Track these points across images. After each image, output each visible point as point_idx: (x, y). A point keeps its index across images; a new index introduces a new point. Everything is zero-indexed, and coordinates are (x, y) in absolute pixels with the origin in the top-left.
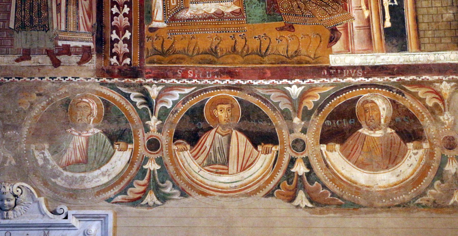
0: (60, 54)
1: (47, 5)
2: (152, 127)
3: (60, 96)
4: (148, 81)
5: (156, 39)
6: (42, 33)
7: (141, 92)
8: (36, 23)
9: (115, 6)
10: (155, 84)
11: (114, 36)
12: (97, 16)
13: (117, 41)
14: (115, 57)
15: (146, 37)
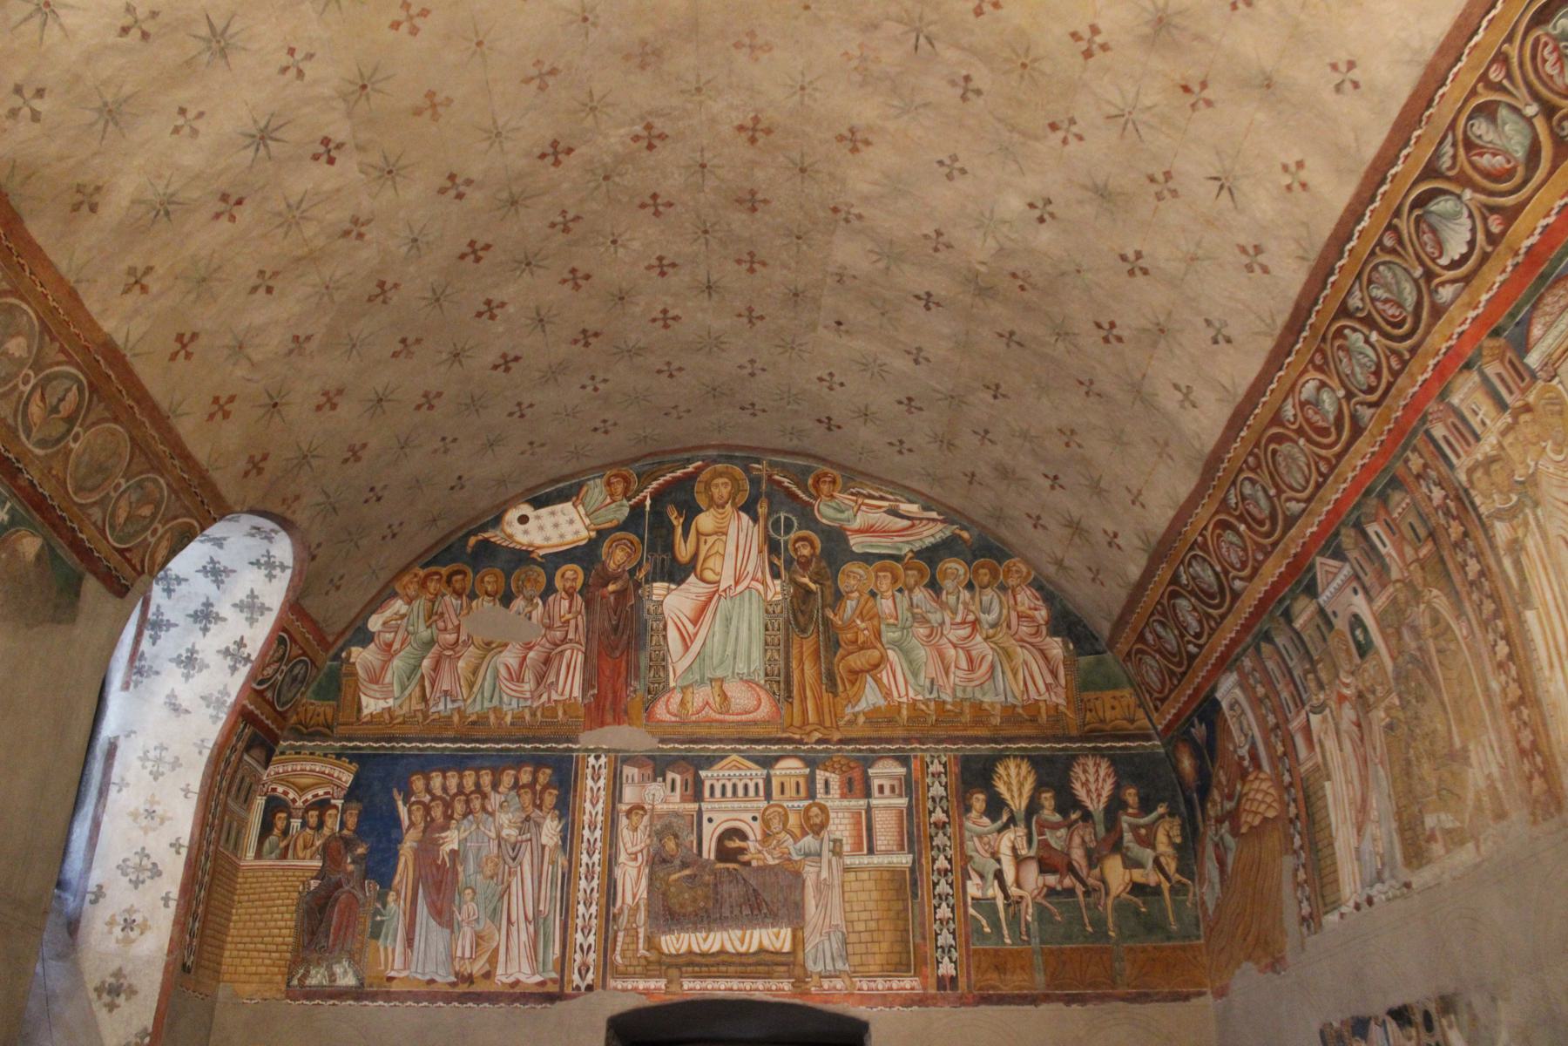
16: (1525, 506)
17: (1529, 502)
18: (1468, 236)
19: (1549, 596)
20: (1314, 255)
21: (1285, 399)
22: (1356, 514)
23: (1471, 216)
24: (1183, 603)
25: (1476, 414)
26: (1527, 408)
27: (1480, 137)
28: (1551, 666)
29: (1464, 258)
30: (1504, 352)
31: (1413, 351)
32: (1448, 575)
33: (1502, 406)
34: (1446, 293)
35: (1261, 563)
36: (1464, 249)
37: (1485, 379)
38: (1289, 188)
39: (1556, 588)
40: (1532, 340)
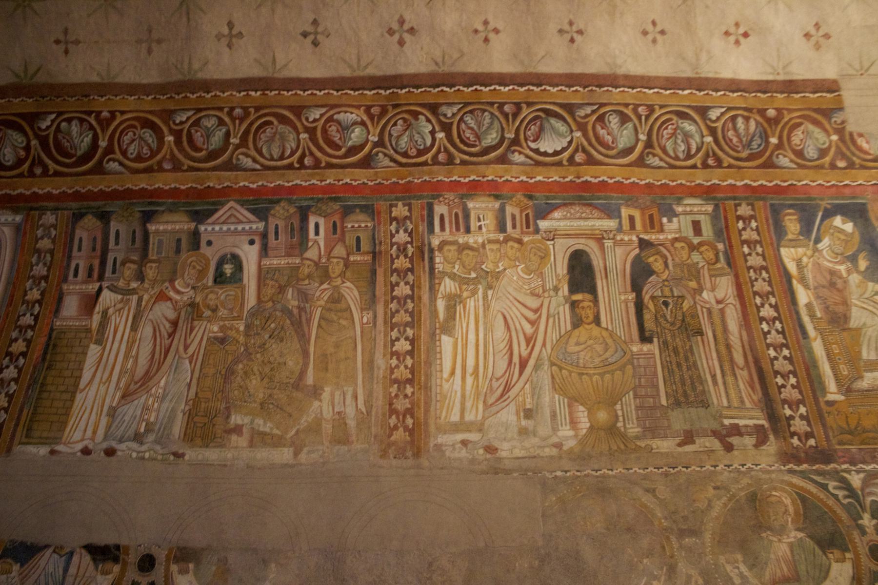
0: (729, 435)
1: (701, 377)
2: (868, 527)
3: (742, 489)
4: (844, 466)
5: (838, 415)
6: (702, 411)
7: (840, 481)
8: (691, 399)
9: (779, 376)
10: (854, 471)
11: (788, 412)
12: (762, 388)
13: (791, 418)
14: (796, 438)
15: (825, 411)
16: (481, 283)
17: (484, 283)
18: (559, 149)
19: (472, 337)
20: (445, 69)
21: (322, 106)
22: (310, 203)
23: (570, 142)
24: (18, 138)
25: (479, 220)
26: (520, 241)
27: (610, 122)
28: (453, 373)
29: (545, 154)
30: (526, 209)
31: (463, 163)
32: (373, 282)
33: (502, 228)
34: (517, 158)
35: (161, 169)
36: (550, 151)
37: (502, 210)
38: (476, 31)
39: (481, 336)
40: (550, 216)
